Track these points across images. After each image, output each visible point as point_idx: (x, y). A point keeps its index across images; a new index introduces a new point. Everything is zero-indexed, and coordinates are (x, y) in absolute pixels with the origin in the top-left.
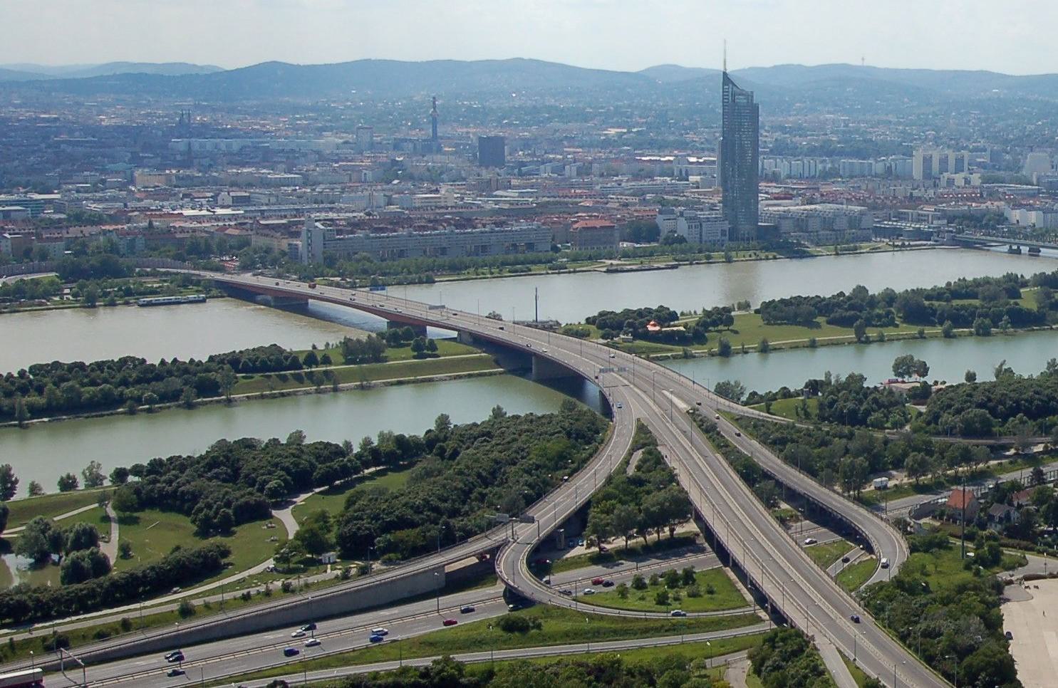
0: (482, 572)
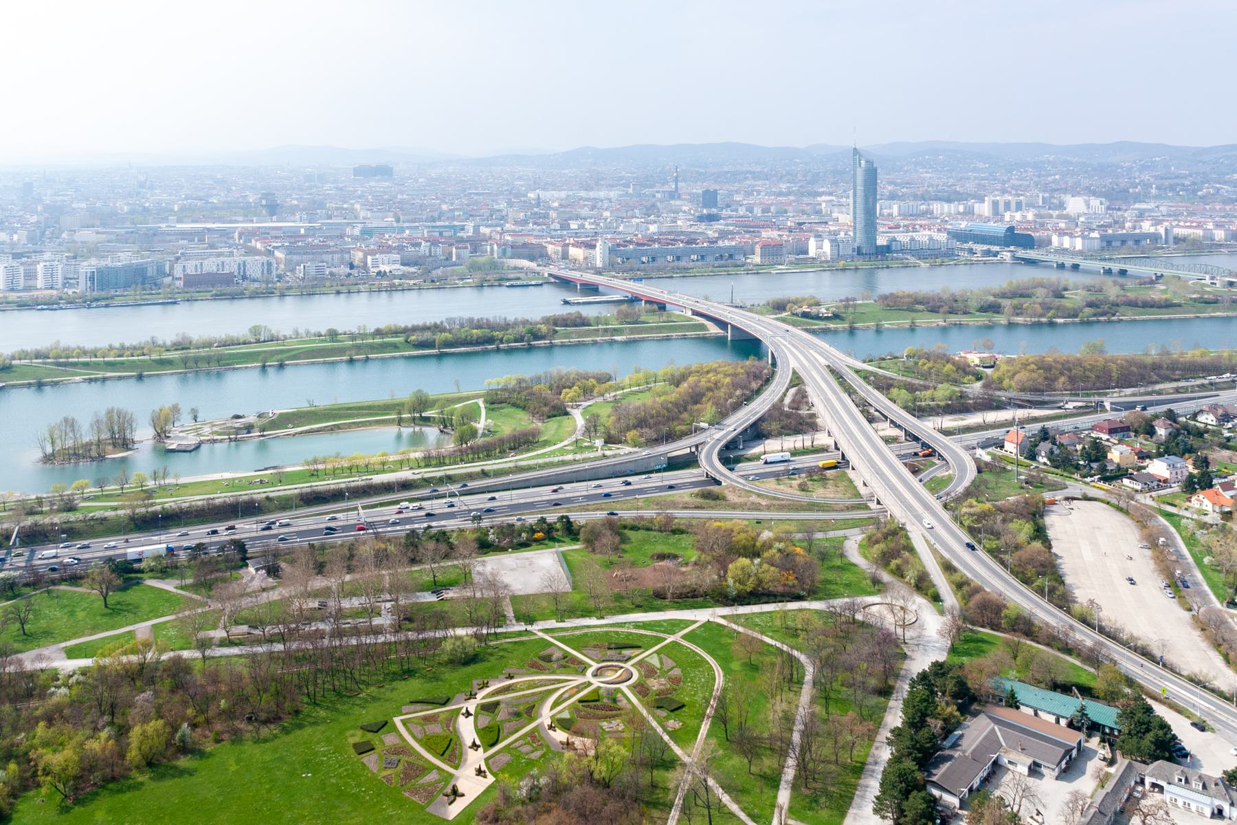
0: (689, 461)
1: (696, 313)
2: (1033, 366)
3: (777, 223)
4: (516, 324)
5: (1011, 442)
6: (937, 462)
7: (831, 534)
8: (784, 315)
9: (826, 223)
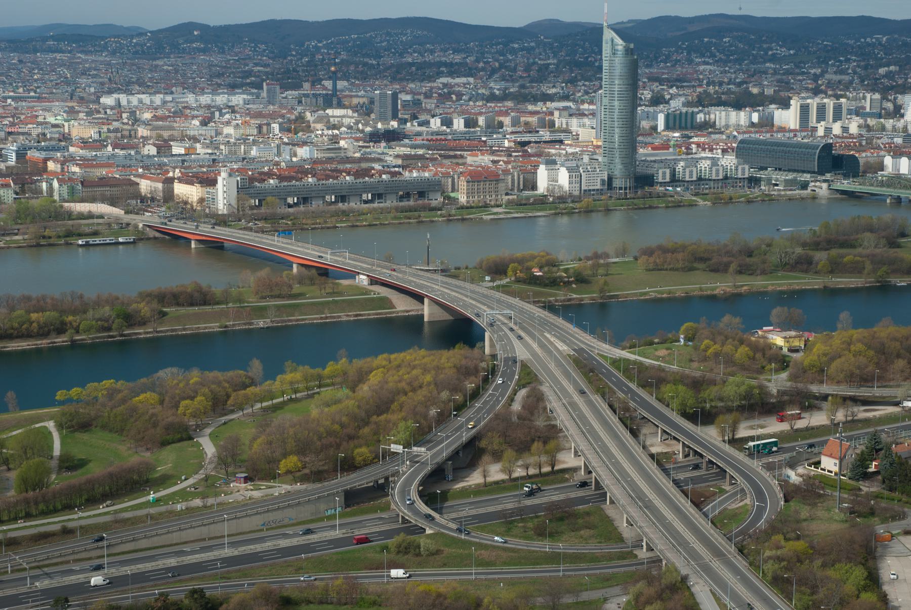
1: (374, 281)
2: (859, 346)
3: (490, 143)
4: (98, 304)
5: (831, 456)
6: (727, 488)
7: (585, 596)
8: (505, 281)
9: (561, 142)
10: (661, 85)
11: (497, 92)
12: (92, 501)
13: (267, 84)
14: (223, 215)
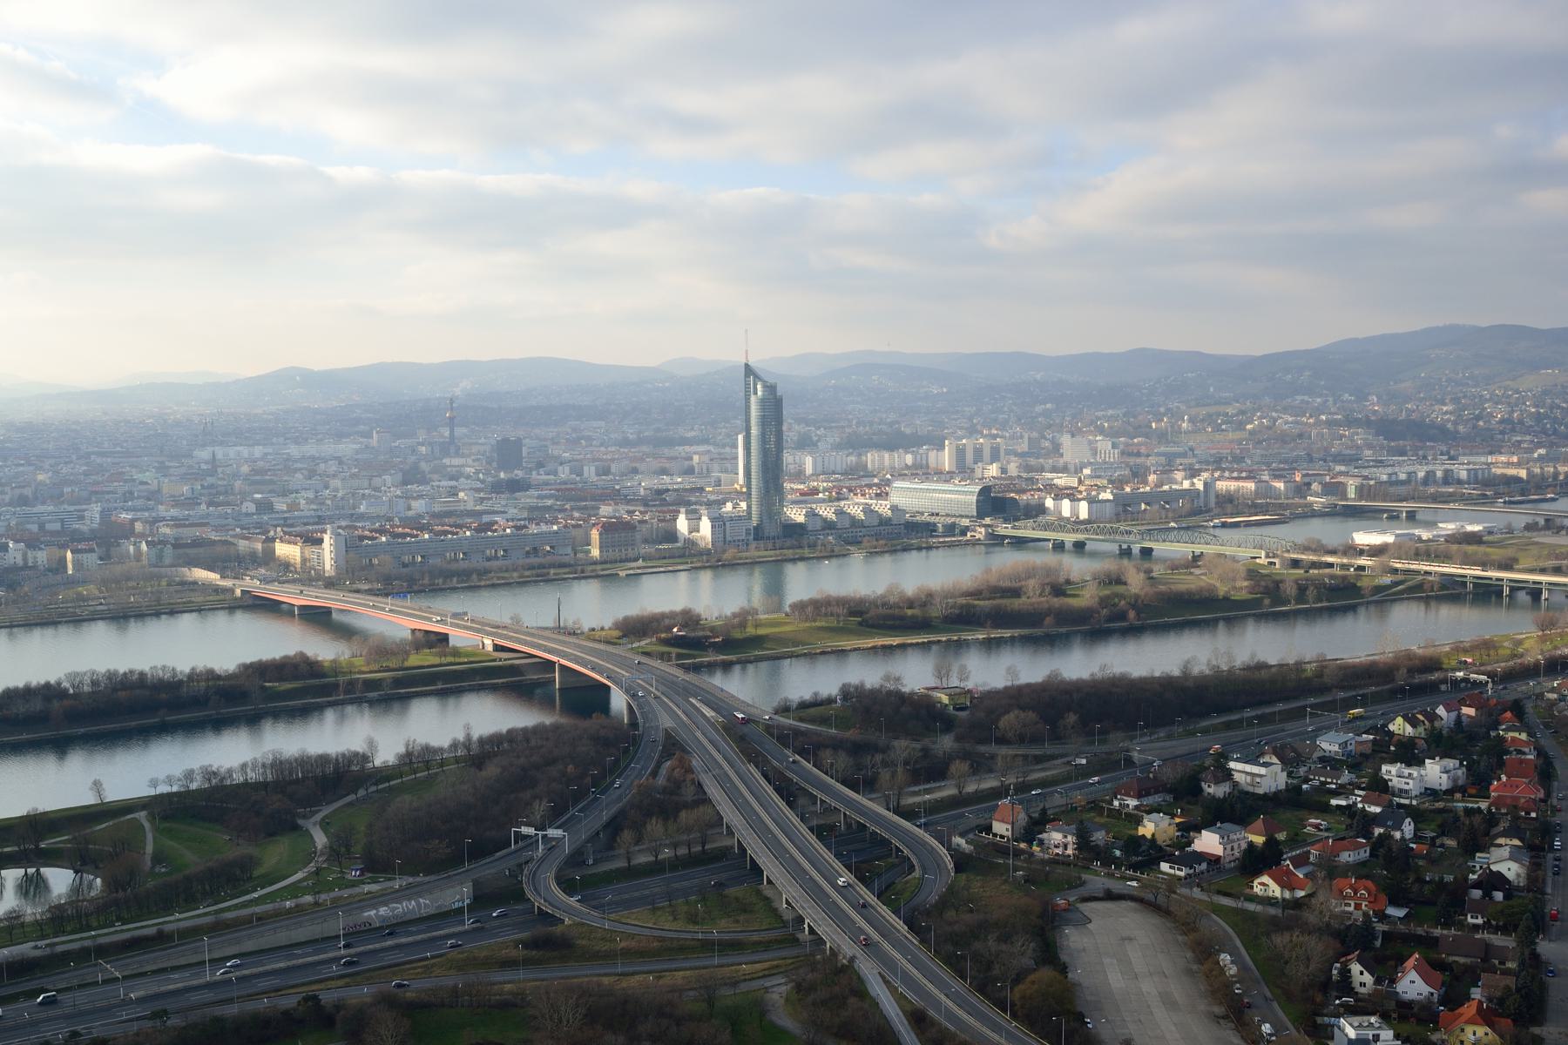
10: (807, 425)
11: (631, 437)
12: (190, 901)
13: (377, 432)
14: (330, 577)
